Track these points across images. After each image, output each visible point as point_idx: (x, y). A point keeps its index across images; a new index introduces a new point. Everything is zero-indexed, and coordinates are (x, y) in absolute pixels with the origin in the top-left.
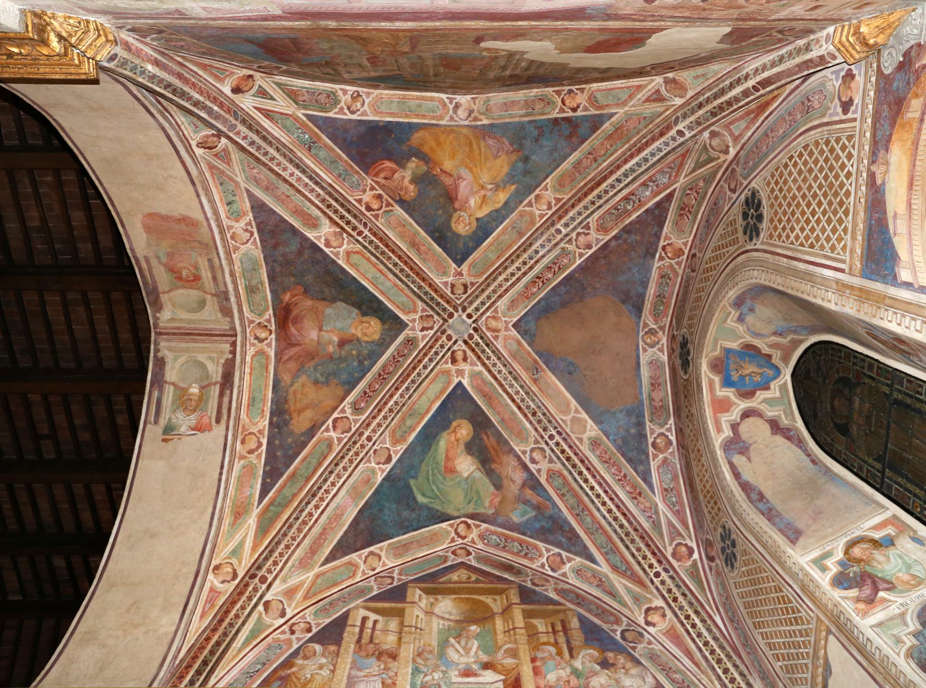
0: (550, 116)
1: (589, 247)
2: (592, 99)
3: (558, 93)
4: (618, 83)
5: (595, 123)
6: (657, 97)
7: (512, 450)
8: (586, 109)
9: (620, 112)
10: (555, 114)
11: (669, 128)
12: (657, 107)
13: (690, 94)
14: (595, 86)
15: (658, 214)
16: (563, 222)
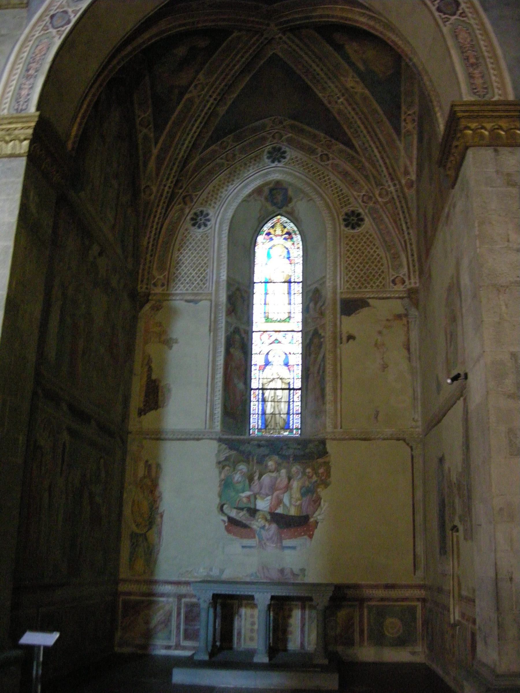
0: (403, 104)
1: (330, 103)
2: (409, 133)
3: (414, 113)
4: (415, 152)
5: (398, 131)
6: (406, 173)
7: (197, 72)
8: (405, 127)
9: (401, 146)
10: (404, 108)
11: (392, 179)
12: (402, 169)
13: (406, 190)
14: (415, 136)
15: (349, 144)
16: (345, 102)
